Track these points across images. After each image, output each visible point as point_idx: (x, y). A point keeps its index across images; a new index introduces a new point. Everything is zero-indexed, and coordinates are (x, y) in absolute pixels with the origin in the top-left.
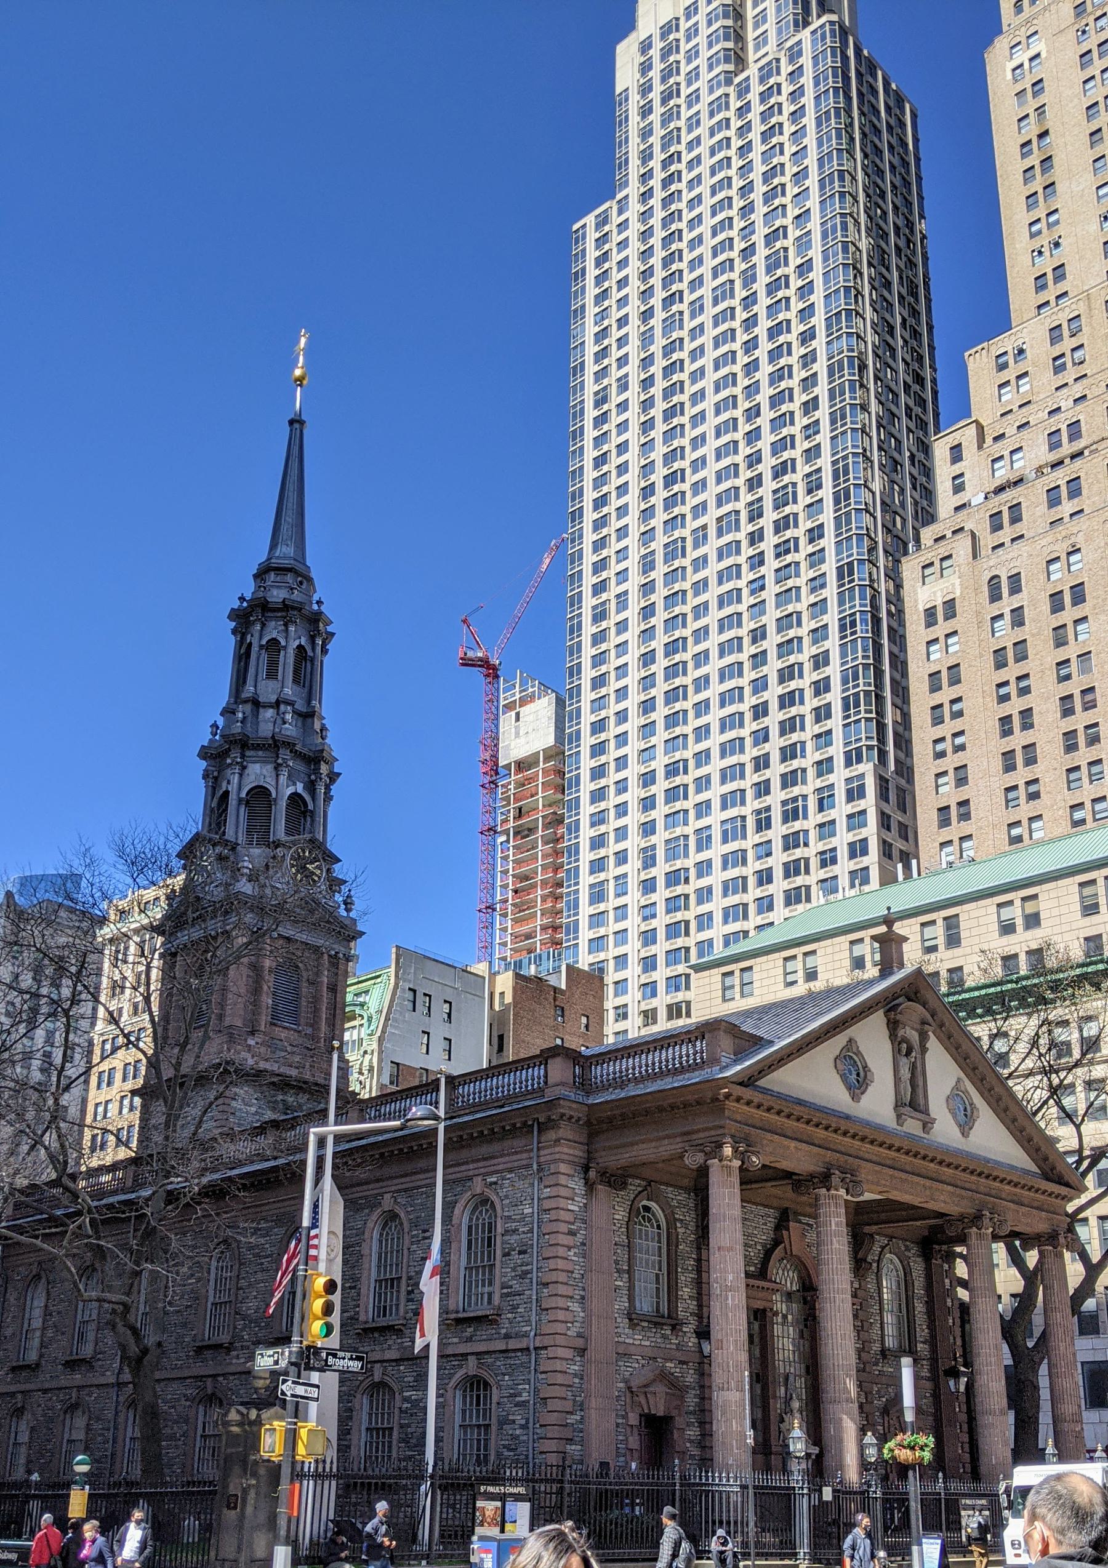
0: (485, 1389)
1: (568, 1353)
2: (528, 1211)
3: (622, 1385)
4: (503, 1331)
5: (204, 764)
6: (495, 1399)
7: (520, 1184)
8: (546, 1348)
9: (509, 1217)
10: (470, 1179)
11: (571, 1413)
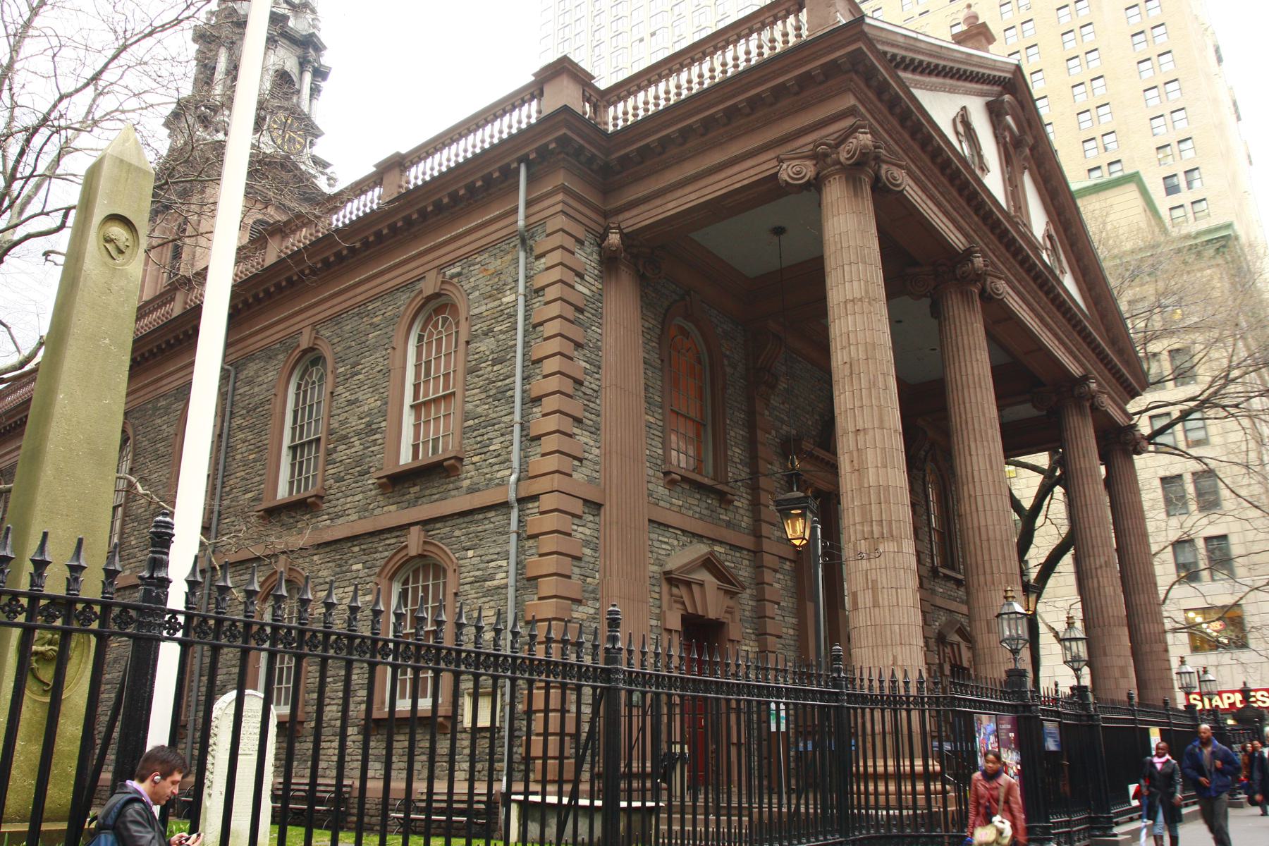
0: (436, 577)
1: (578, 507)
2: (508, 298)
3: (655, 568)
4: (466, 483)
5: (196, 47)
6: (451, 590)
7: (495, 264)
8: (535, 498)
9: (478, 316)
10: (421, 278)
11: (578, 602)
